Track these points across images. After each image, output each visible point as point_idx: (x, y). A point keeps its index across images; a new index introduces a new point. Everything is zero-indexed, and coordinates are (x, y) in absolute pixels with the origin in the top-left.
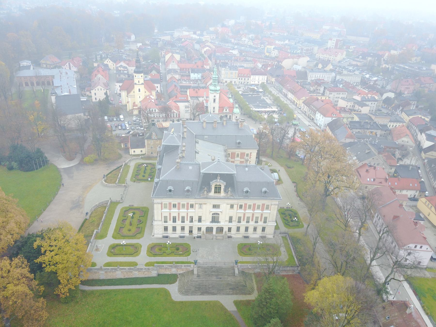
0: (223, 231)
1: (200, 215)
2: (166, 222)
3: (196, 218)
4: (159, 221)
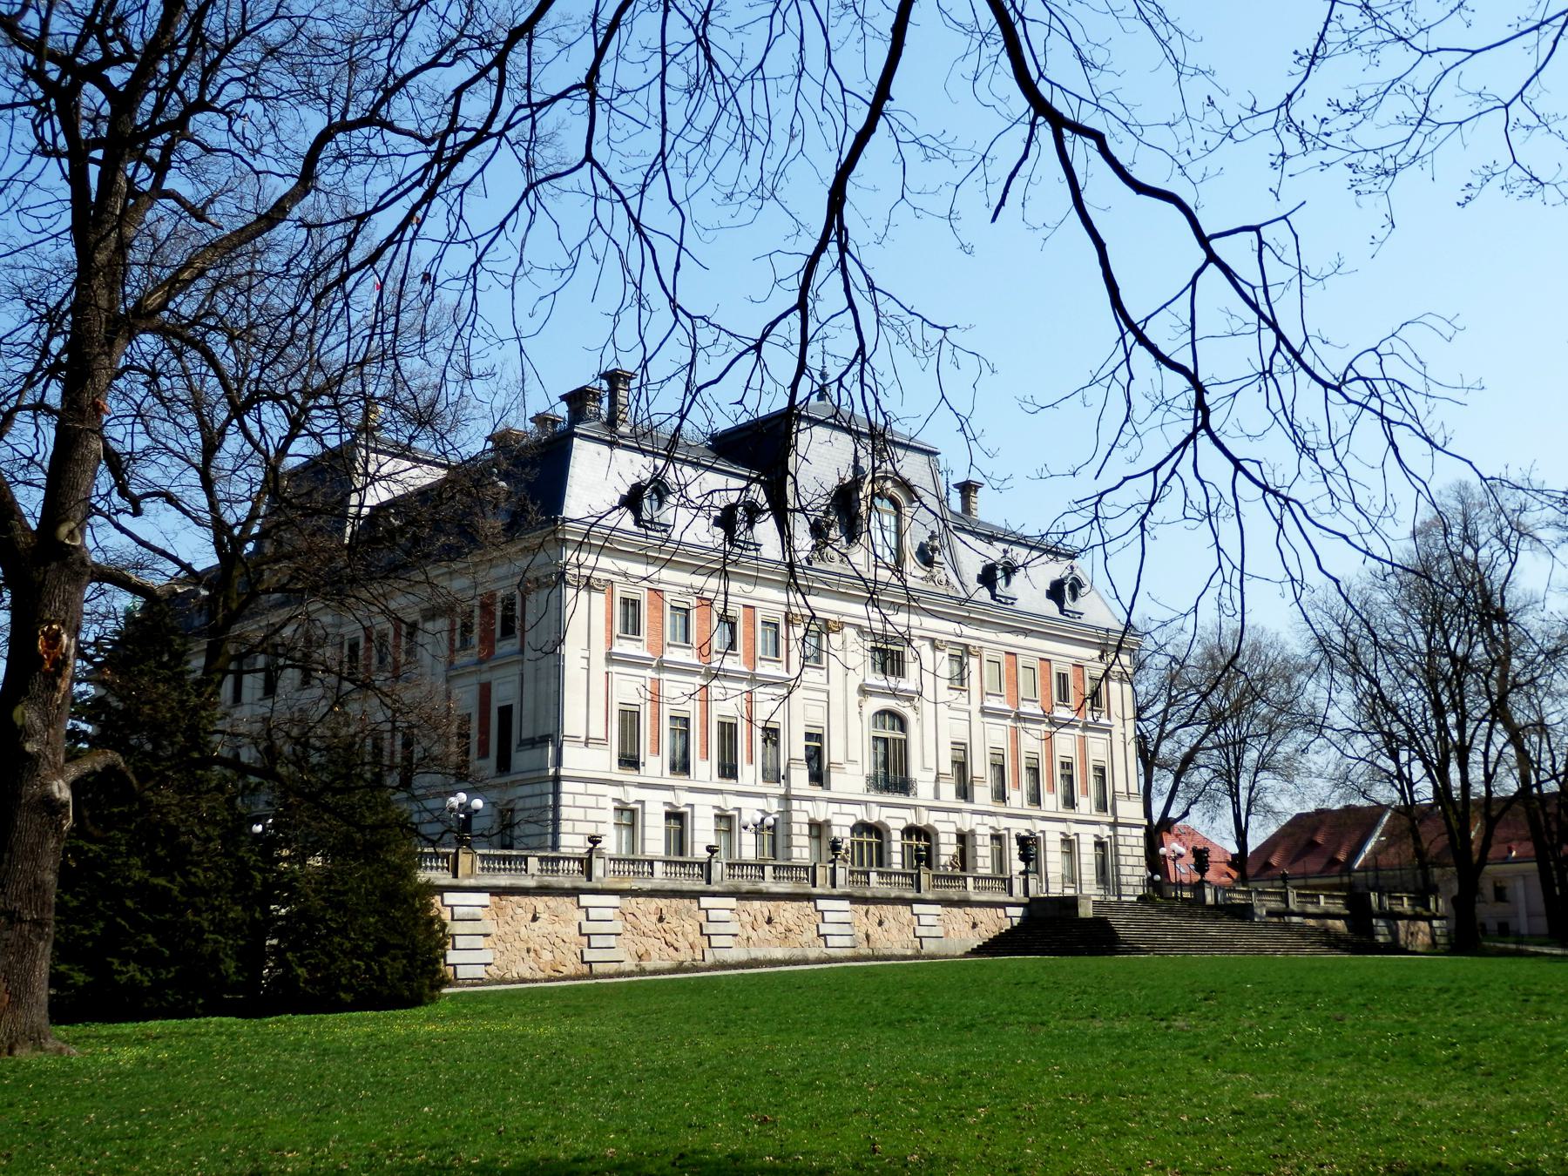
2: (630, 761)
3: (795, 746)
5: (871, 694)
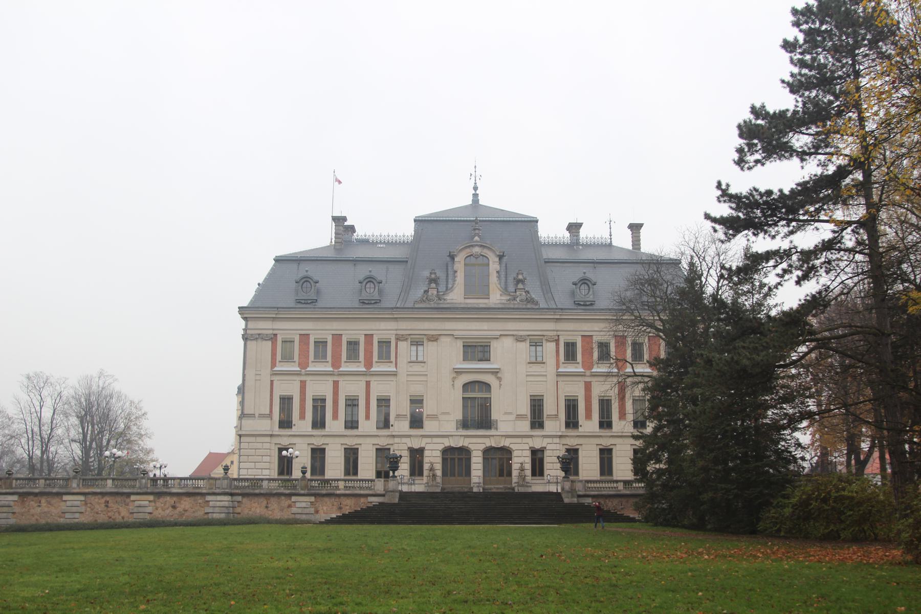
0: (510, 474)
1: (416, 390)
2: (286, 423)
3: (400, 407)
4: (262, 416)
5: (461, 373)
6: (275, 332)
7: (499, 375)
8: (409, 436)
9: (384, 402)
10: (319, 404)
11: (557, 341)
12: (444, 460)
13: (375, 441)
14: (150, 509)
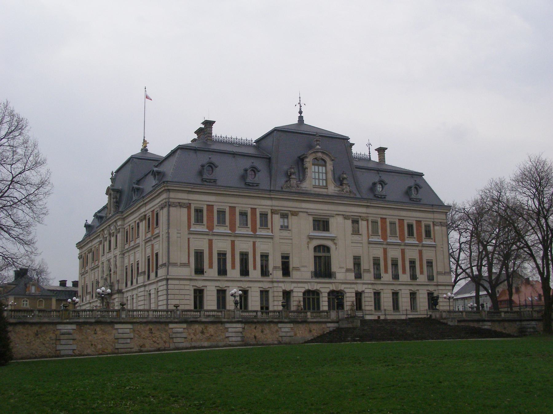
1: (286, 249)
2: (199, 271)
3: (275, 262)
4: (183, 265)
5: (313, 239)
6: (190, 202)
7: (335, 241)
8: (283, 282)
9: (265, 257)
10: (222, 256)
11: (367, 220)
12: (304, 299)
13: (260, 285)
14: (184, 335)
